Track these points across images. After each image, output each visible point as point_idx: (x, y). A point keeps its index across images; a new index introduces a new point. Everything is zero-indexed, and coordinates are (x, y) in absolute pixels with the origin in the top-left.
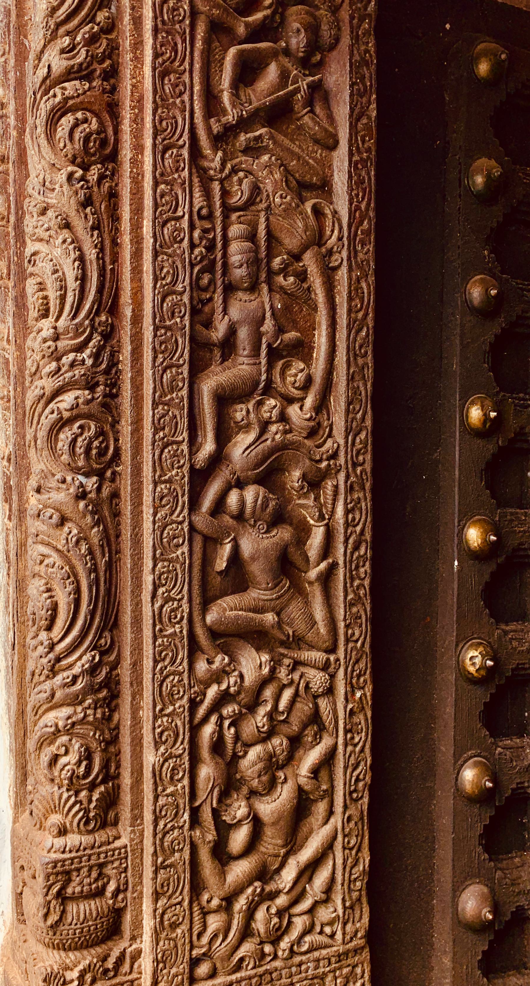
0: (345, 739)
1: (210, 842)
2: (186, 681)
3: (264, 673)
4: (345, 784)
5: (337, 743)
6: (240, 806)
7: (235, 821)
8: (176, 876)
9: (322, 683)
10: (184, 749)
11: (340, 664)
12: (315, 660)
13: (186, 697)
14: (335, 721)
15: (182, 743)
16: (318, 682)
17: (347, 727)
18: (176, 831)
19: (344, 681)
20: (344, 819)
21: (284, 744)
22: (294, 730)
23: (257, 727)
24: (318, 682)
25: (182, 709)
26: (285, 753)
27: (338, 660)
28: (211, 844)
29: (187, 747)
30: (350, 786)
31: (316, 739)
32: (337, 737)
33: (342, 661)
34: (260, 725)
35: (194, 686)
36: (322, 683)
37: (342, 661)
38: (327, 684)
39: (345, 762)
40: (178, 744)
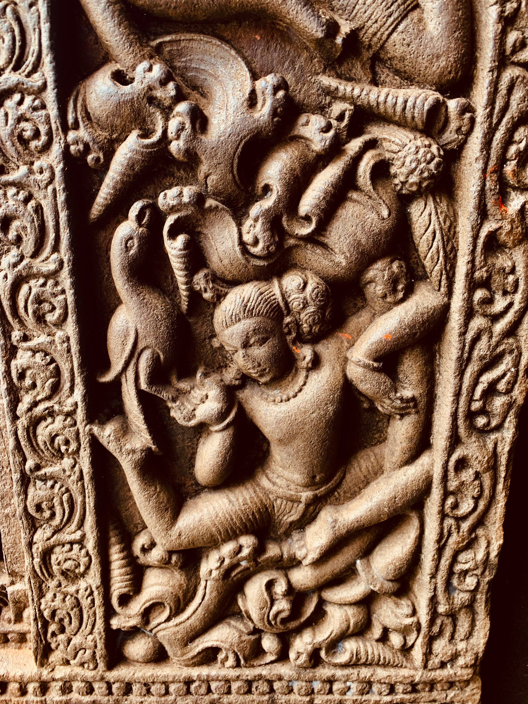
0: (469, 300)
1: (134, 451)
2: (52, 110)
3: (257, 115)
4: (457, 395)
5: (446, 308)
6: (207, 397)
7: (193, 423)
8: (65, 497)
9: (419, 162)
10: (61, 263)
11: (472, 121)
12: (406, 102)
13: (56, 149)
14: (446, 257)
15: (56, 249)
16: (408, 160)
17: (477, 274)
18: (59, 419)
19: (480, 165)
20: (447, 462)
21: (309, 288)
22: (338, 264)
23: (242, 243)
24: (408, 160)
25: (47, 175)
26: (311, 309)
27: (467, 109)
28: (137, 456)
29: (65, 259)
30: (471, 400)
31: (394, 291)
32: (450, 293)
33: (481, 113)
34: (248, 238)
35: (76, 126)
36: (419, 162)
37: (481, 113)
38: (432, 166)
39: (462, 349)
40: (48, 249)
